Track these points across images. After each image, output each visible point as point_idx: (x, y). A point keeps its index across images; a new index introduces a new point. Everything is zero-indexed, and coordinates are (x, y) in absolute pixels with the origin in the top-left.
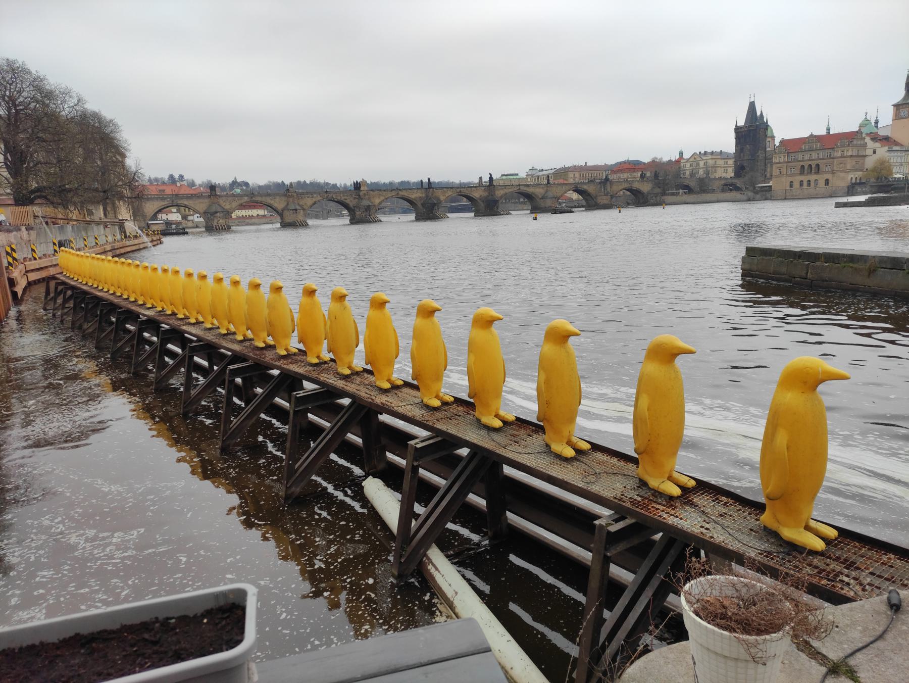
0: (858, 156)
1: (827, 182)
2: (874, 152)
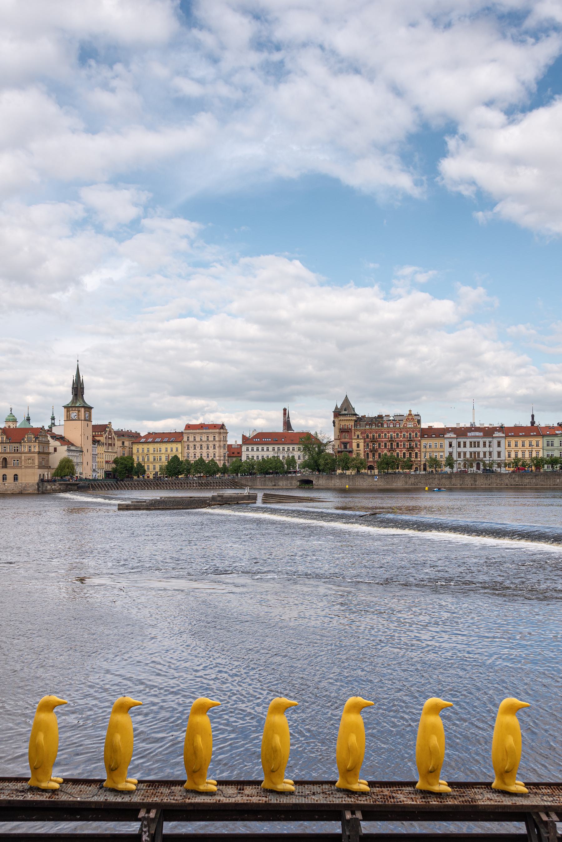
0: (43, 453)
1: (16, 478)
2: (55, 450)
